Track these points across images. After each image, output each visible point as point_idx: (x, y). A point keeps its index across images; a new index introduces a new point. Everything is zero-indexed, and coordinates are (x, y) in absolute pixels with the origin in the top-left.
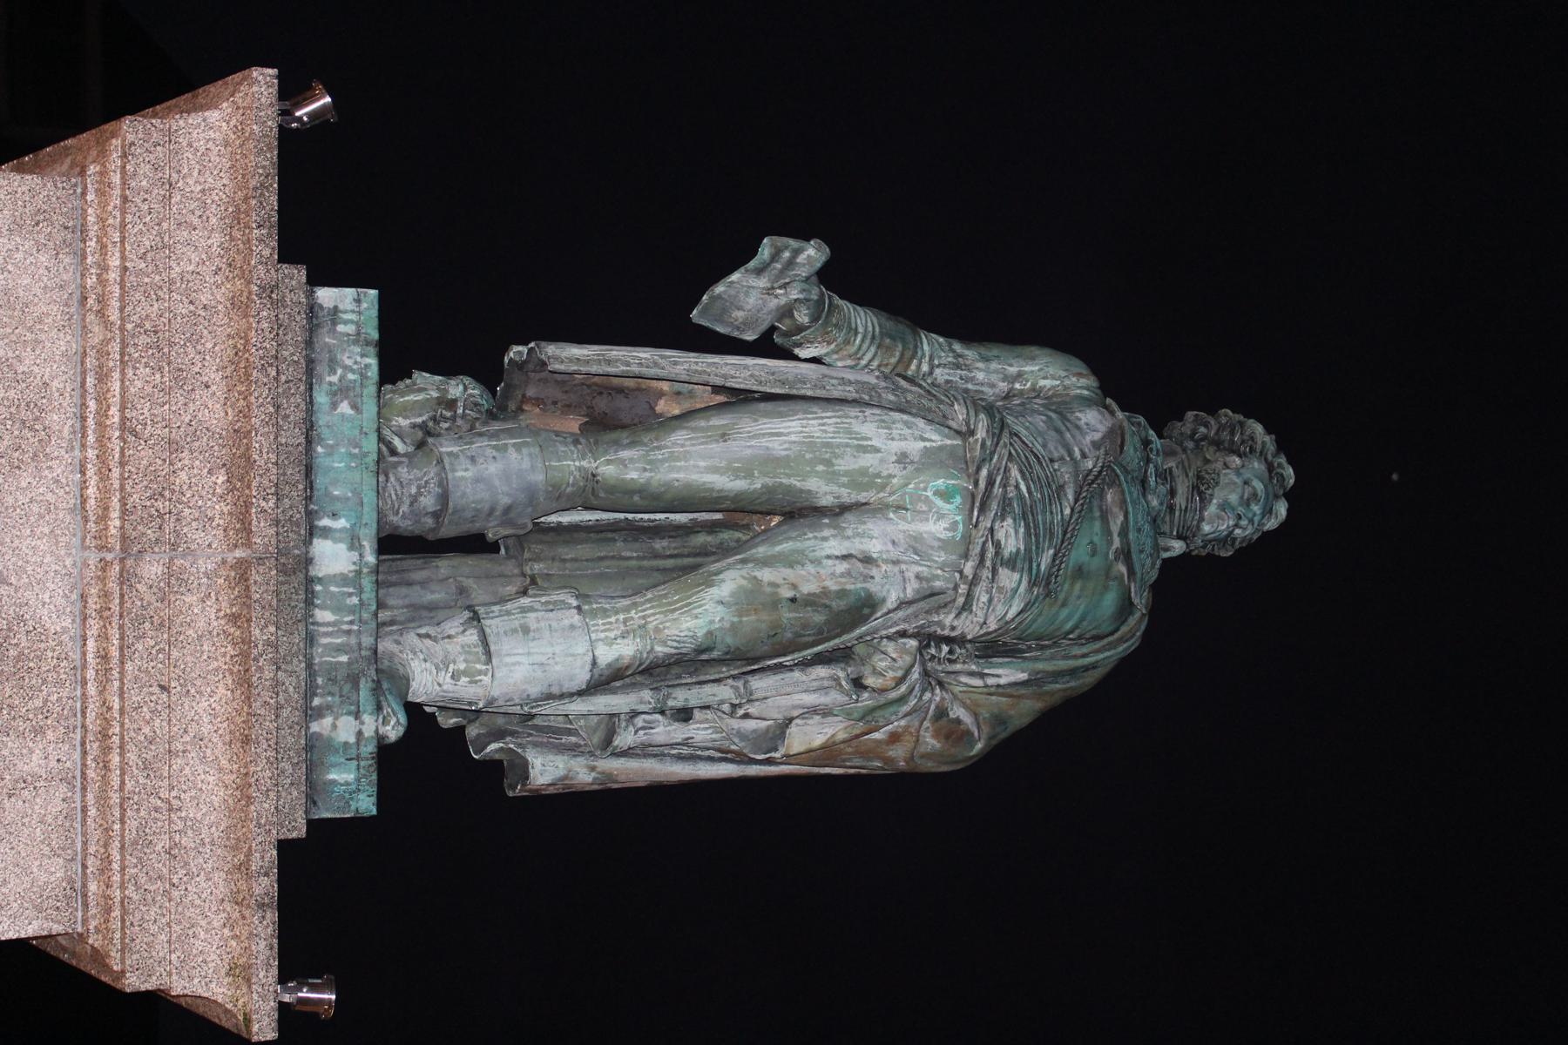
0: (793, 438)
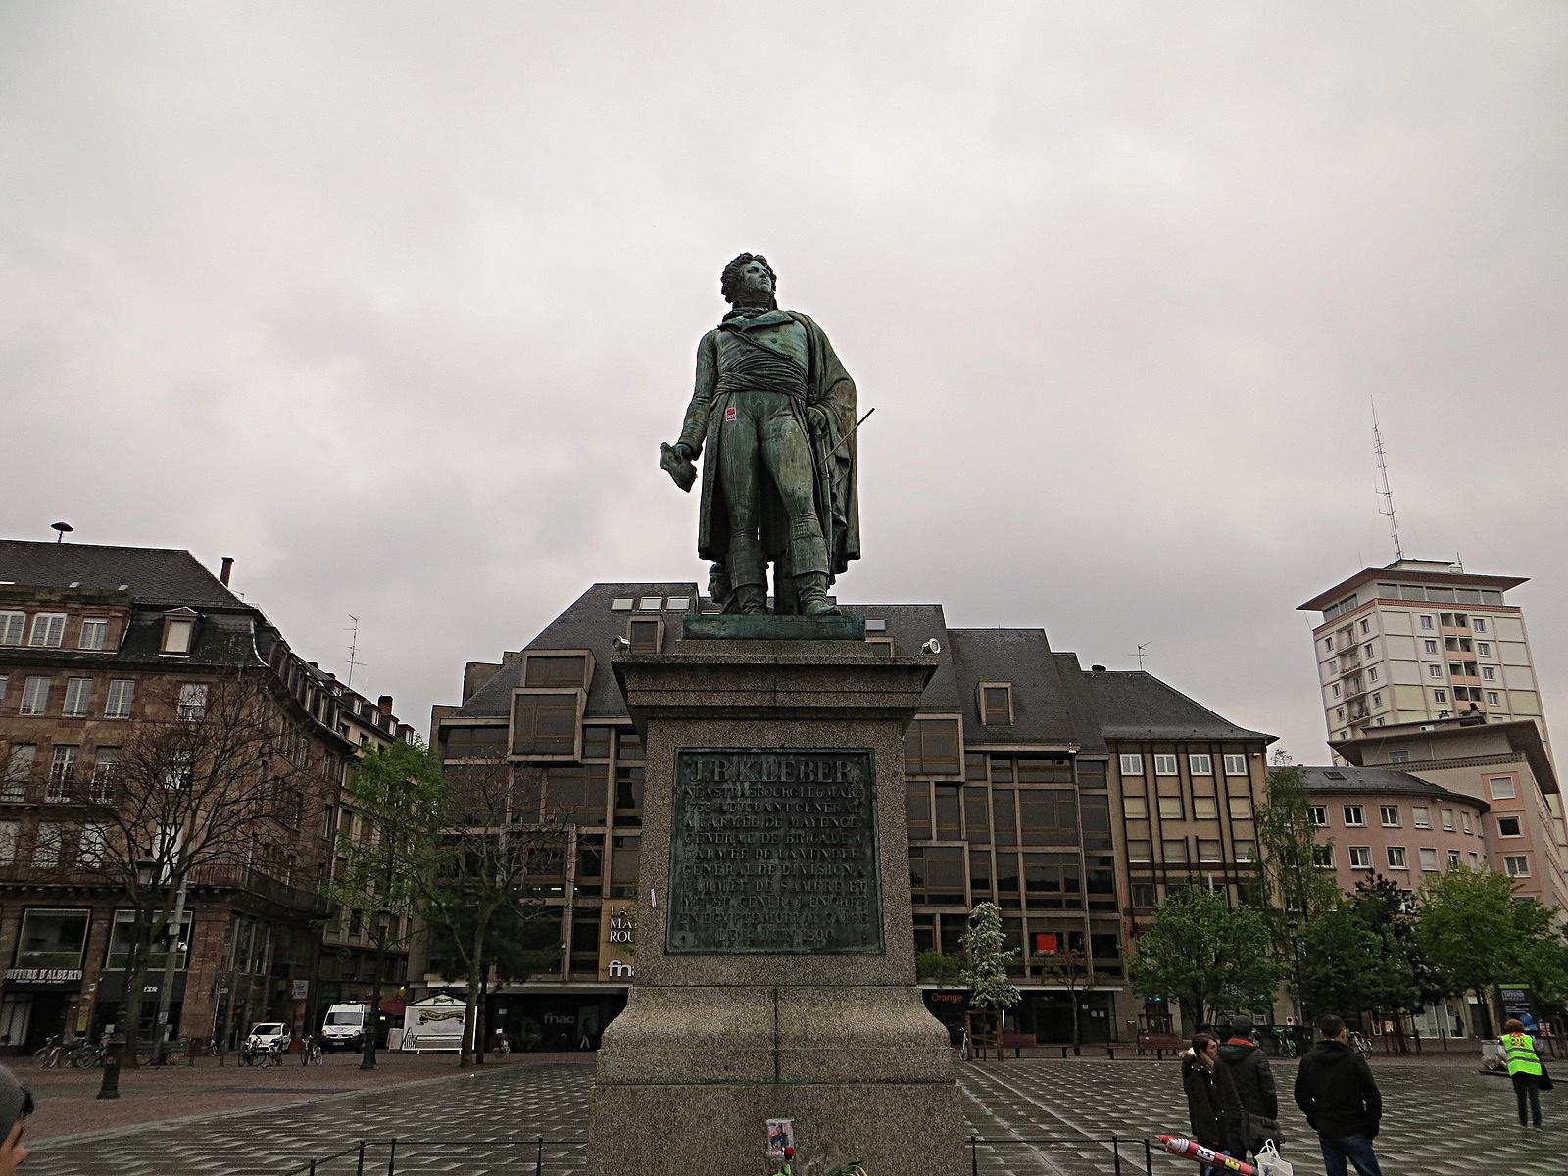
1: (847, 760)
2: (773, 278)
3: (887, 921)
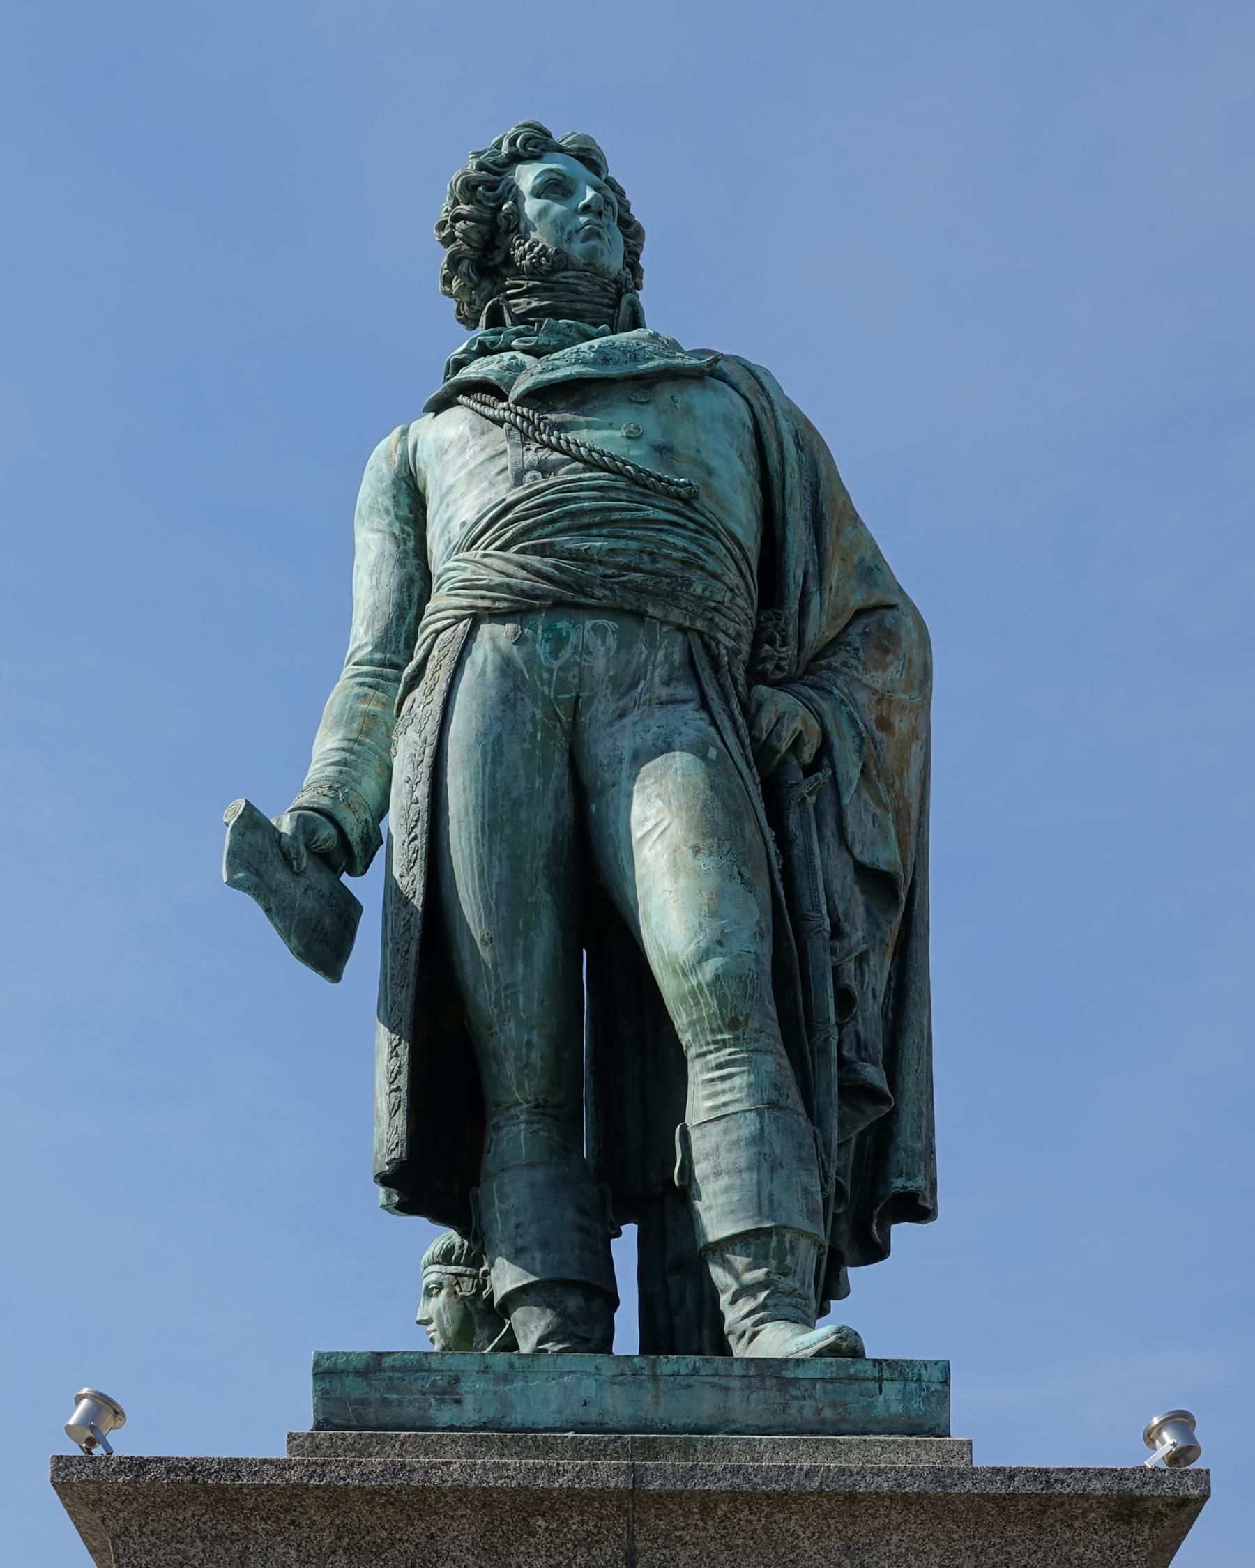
2: (631, 232)
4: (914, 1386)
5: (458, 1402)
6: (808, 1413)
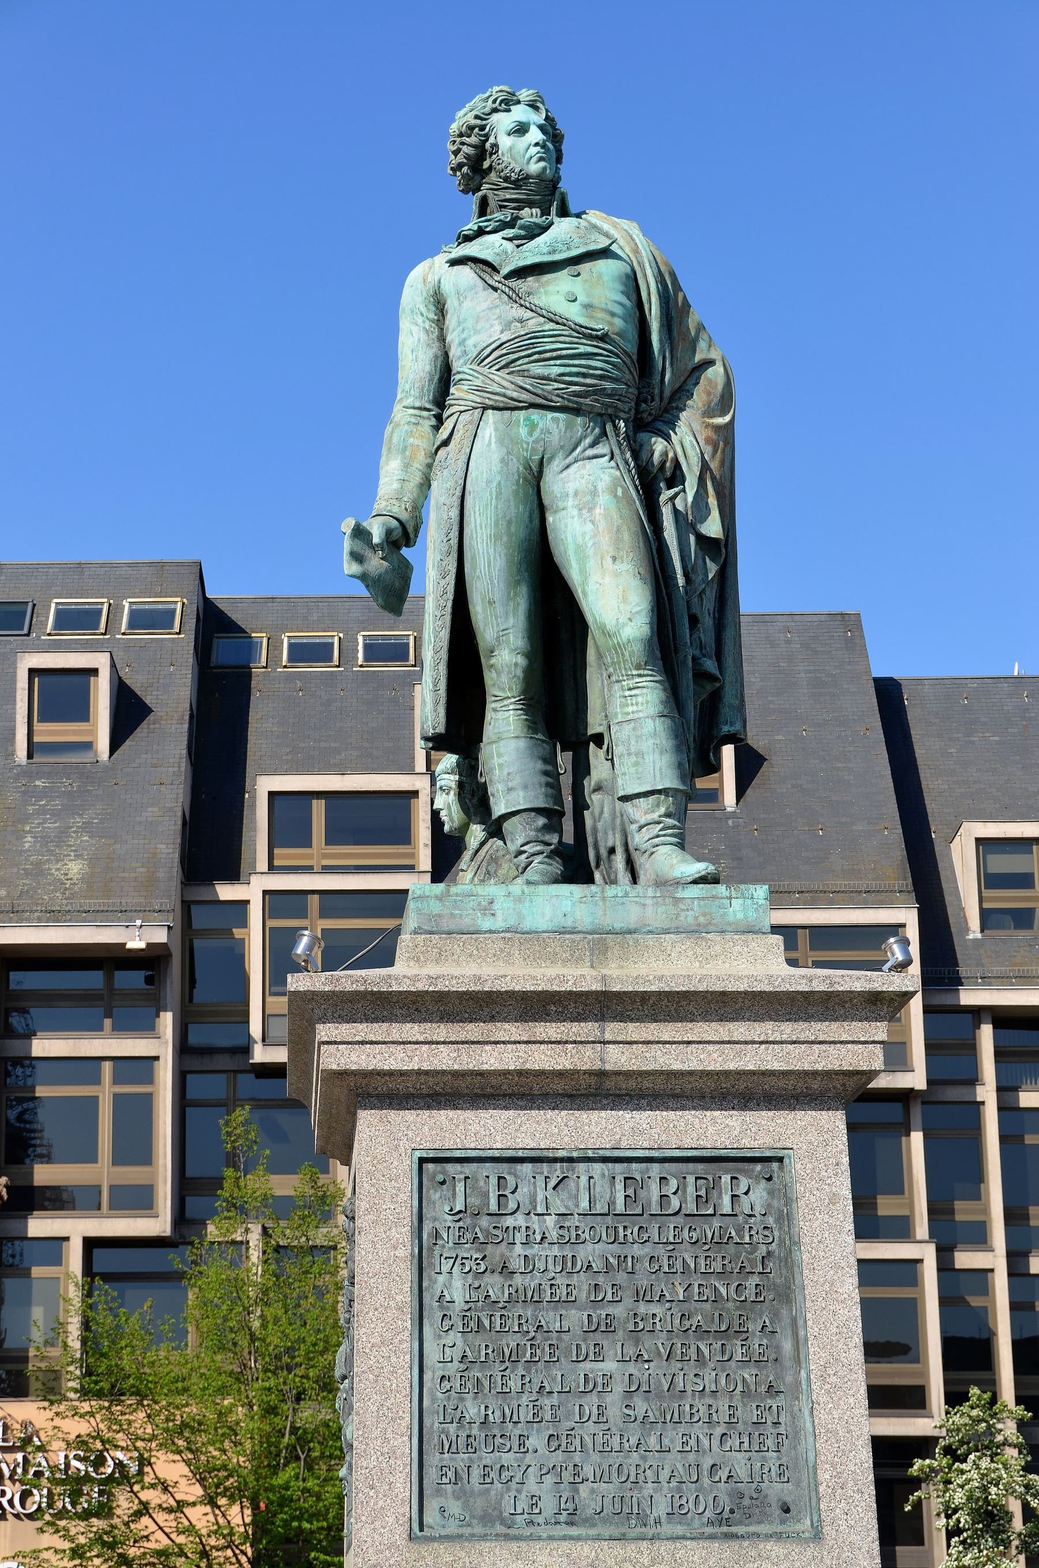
0: (491, 551)
1: (739, 1171)
3: (824, 1476)
4: (749, 902)
5: (493, 915)
6: (690, 920)
